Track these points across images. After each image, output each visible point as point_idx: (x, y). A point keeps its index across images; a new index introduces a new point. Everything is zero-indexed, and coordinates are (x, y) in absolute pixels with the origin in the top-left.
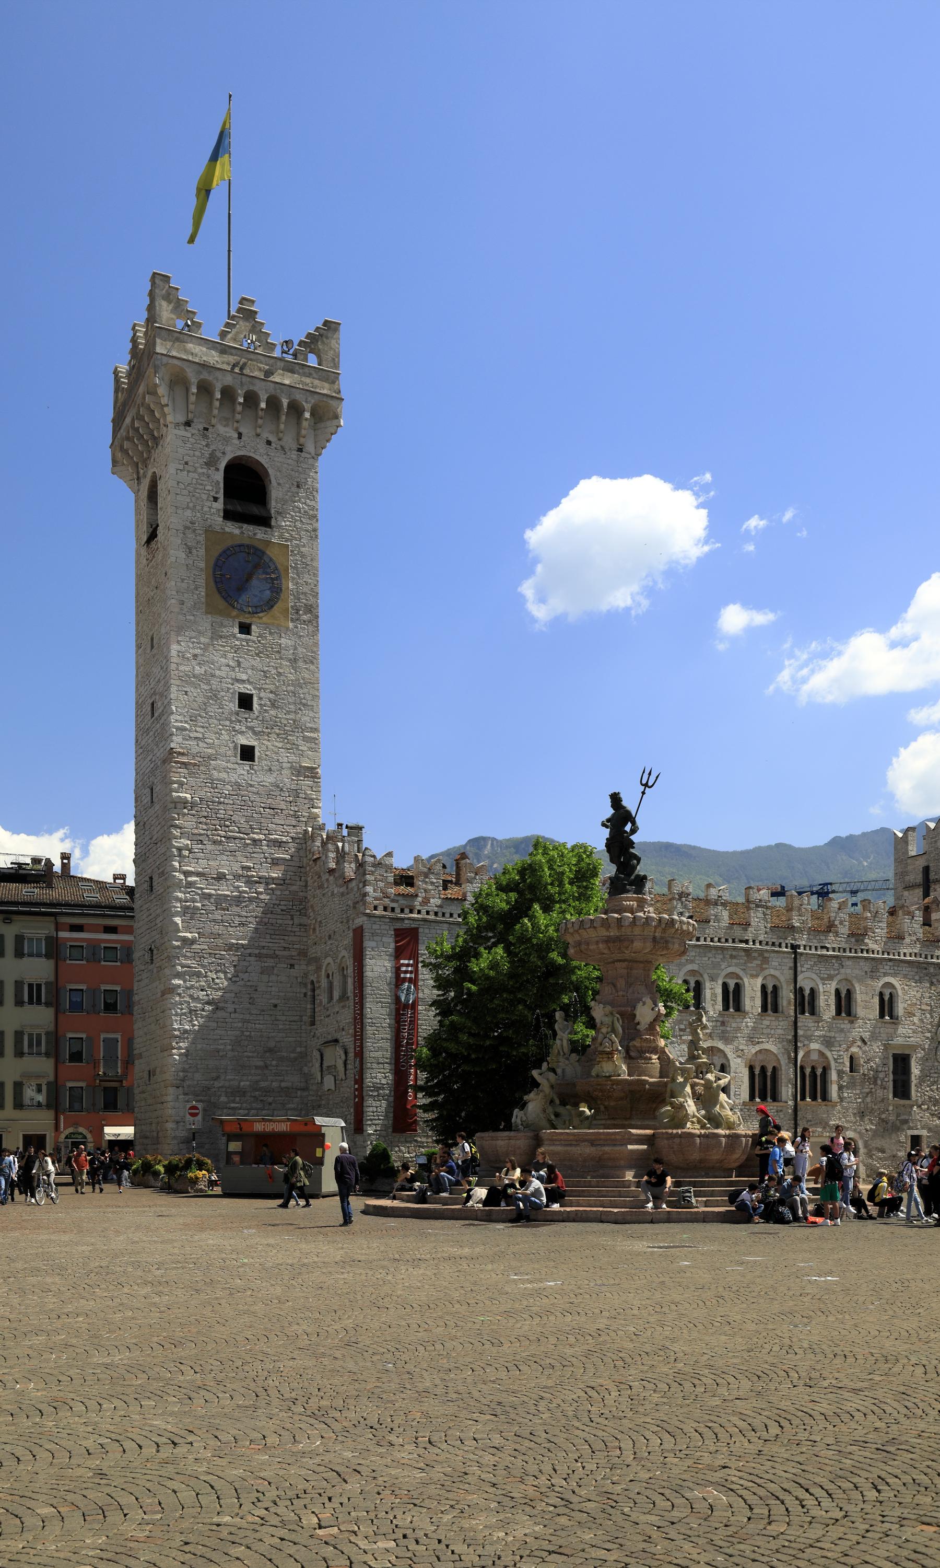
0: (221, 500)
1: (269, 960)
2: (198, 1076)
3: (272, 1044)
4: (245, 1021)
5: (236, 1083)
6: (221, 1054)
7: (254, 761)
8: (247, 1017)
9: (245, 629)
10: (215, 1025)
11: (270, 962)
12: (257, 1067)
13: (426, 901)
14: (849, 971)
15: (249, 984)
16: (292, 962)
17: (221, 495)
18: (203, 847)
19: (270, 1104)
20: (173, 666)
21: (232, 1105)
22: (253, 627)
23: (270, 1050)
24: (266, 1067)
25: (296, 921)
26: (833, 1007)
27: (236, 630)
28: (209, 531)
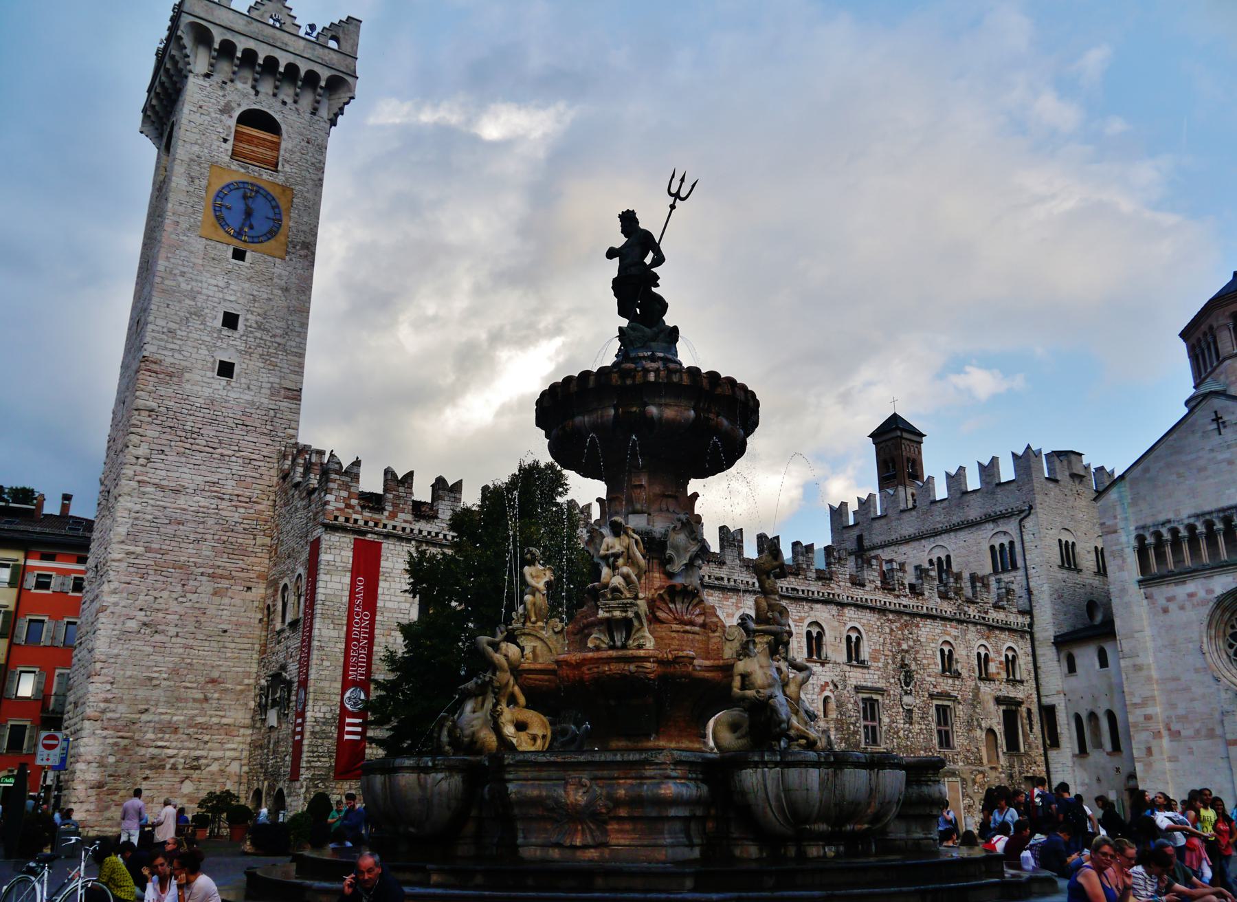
0: (231, 142)
1: (223, 581)
2: (122, 708)
3: (215, 674)
4: (186, 647)
5: (167, 717)
6: (155, 682)
7: (231, 377)
8: (191, 642)
9: (239, 255)
10: (150, 649)
11: (225, 583)
12: (195, 700)
13: (393, 516)
14: (818, 614)
15: (197, 605)
16: (250, 584)
17: (231, 138)
18: (162, 457)
19: (206, 743)
20: (157, 280)
21: (160, 743)
22: (248, 254)
23: (213, 681)
24: (206, 699)
25: (259, 541)
26: (805, 650)
27: (230, 253)
28: (214, 165)
